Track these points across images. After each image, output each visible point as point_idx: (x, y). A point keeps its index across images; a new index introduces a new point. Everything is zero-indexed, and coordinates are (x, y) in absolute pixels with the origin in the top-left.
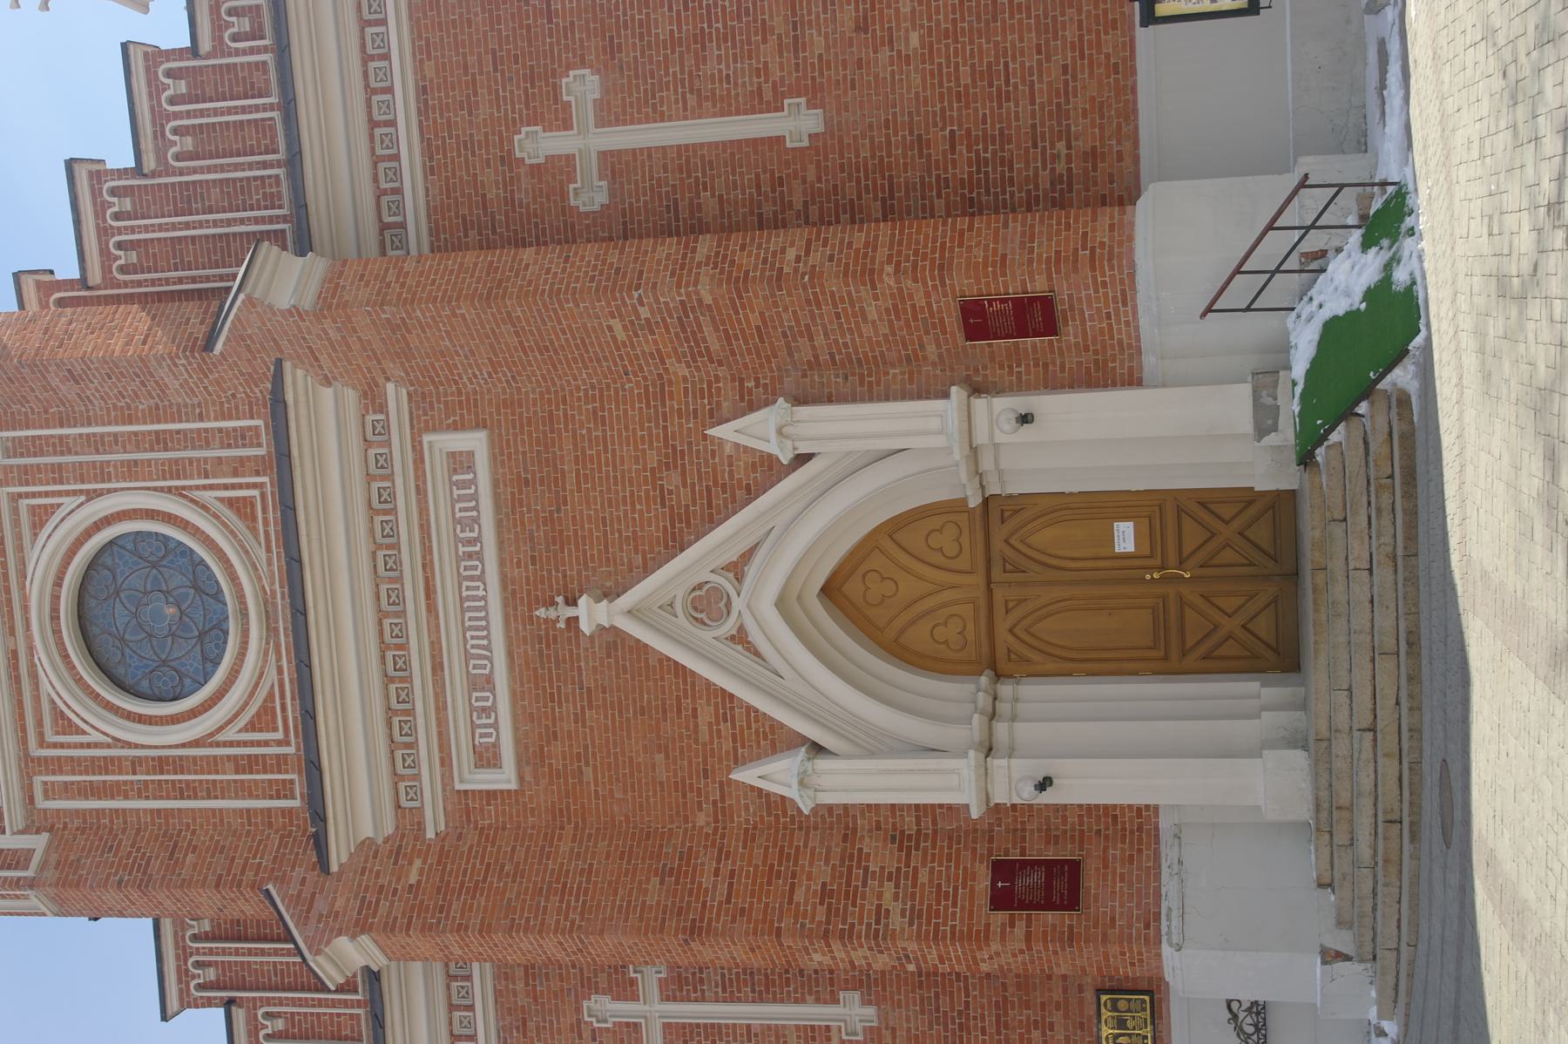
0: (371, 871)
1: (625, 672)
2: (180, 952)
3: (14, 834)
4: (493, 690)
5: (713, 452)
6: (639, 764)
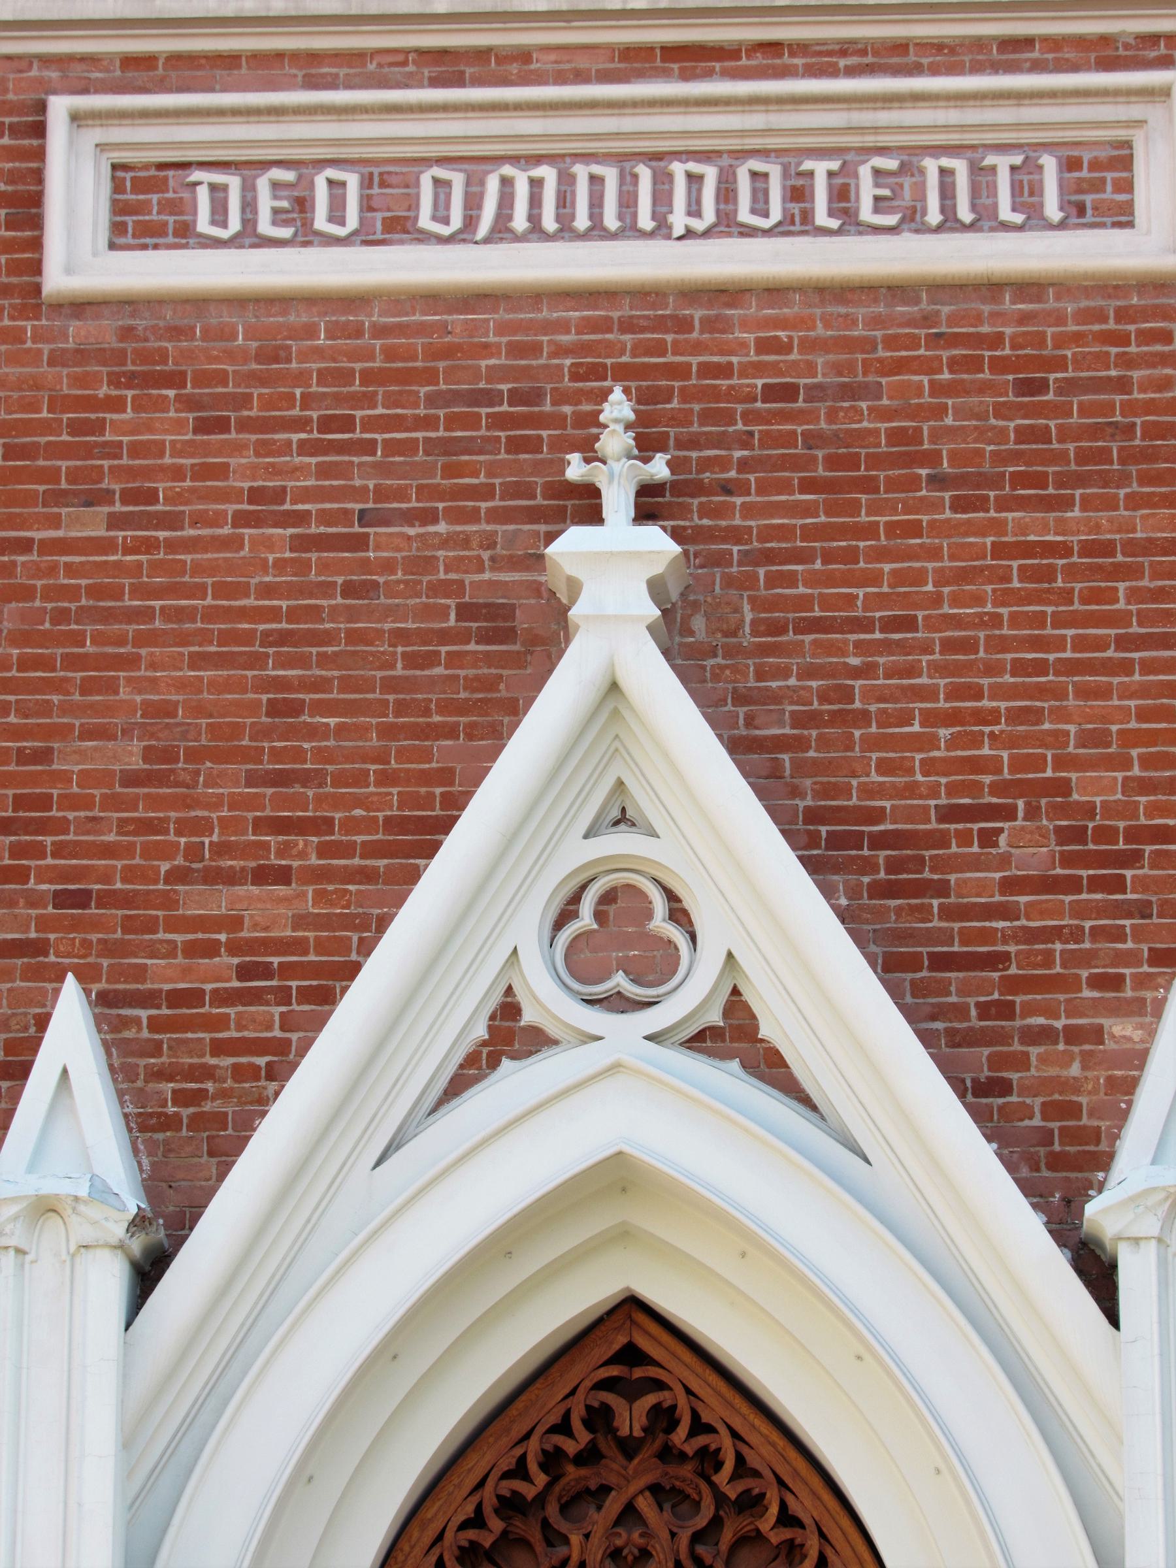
1: (411, 661)
4: (364, 237)
5: (1116, 982)
6: (111, 687)
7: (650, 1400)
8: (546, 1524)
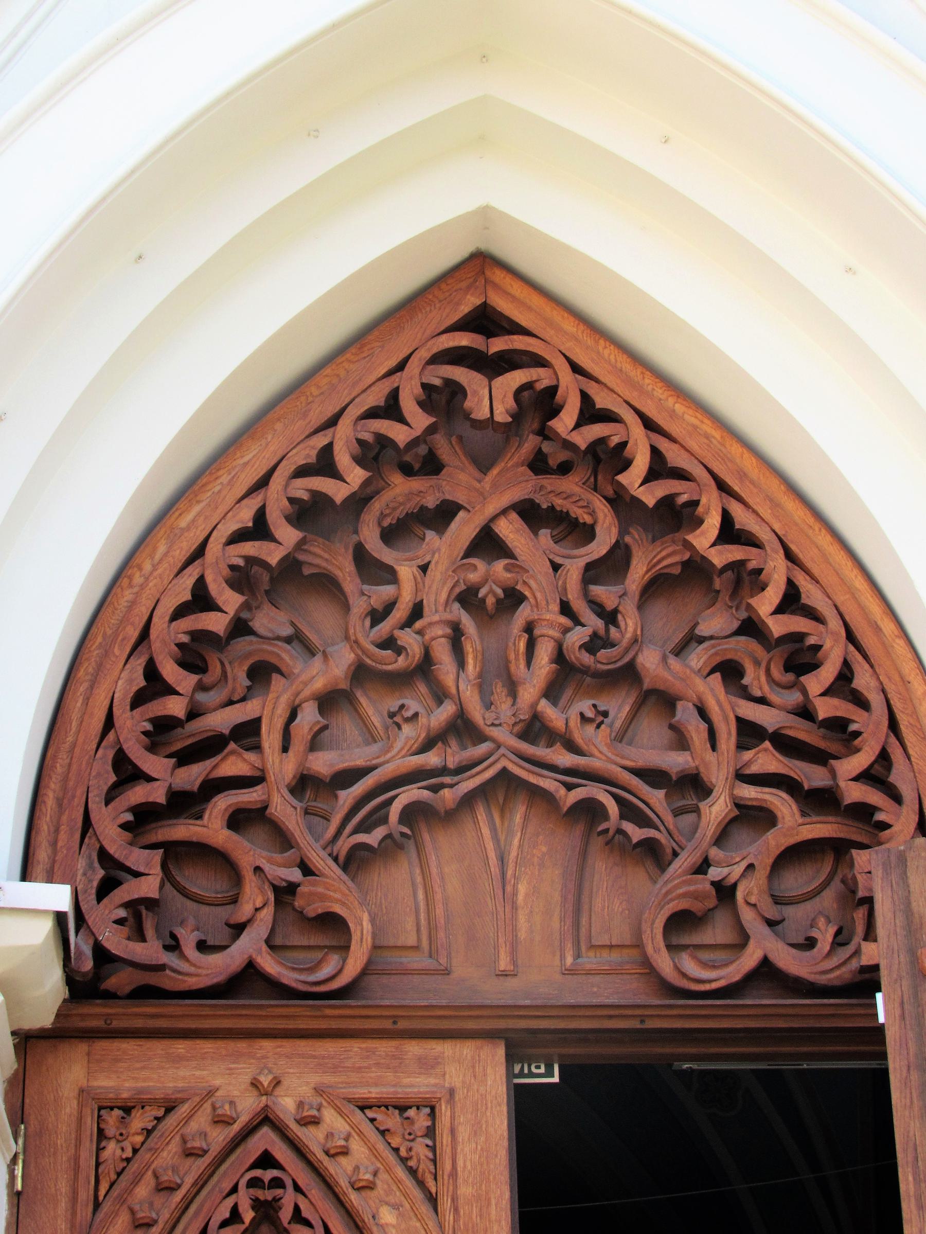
7: (517, 378)
8: (361, 556)
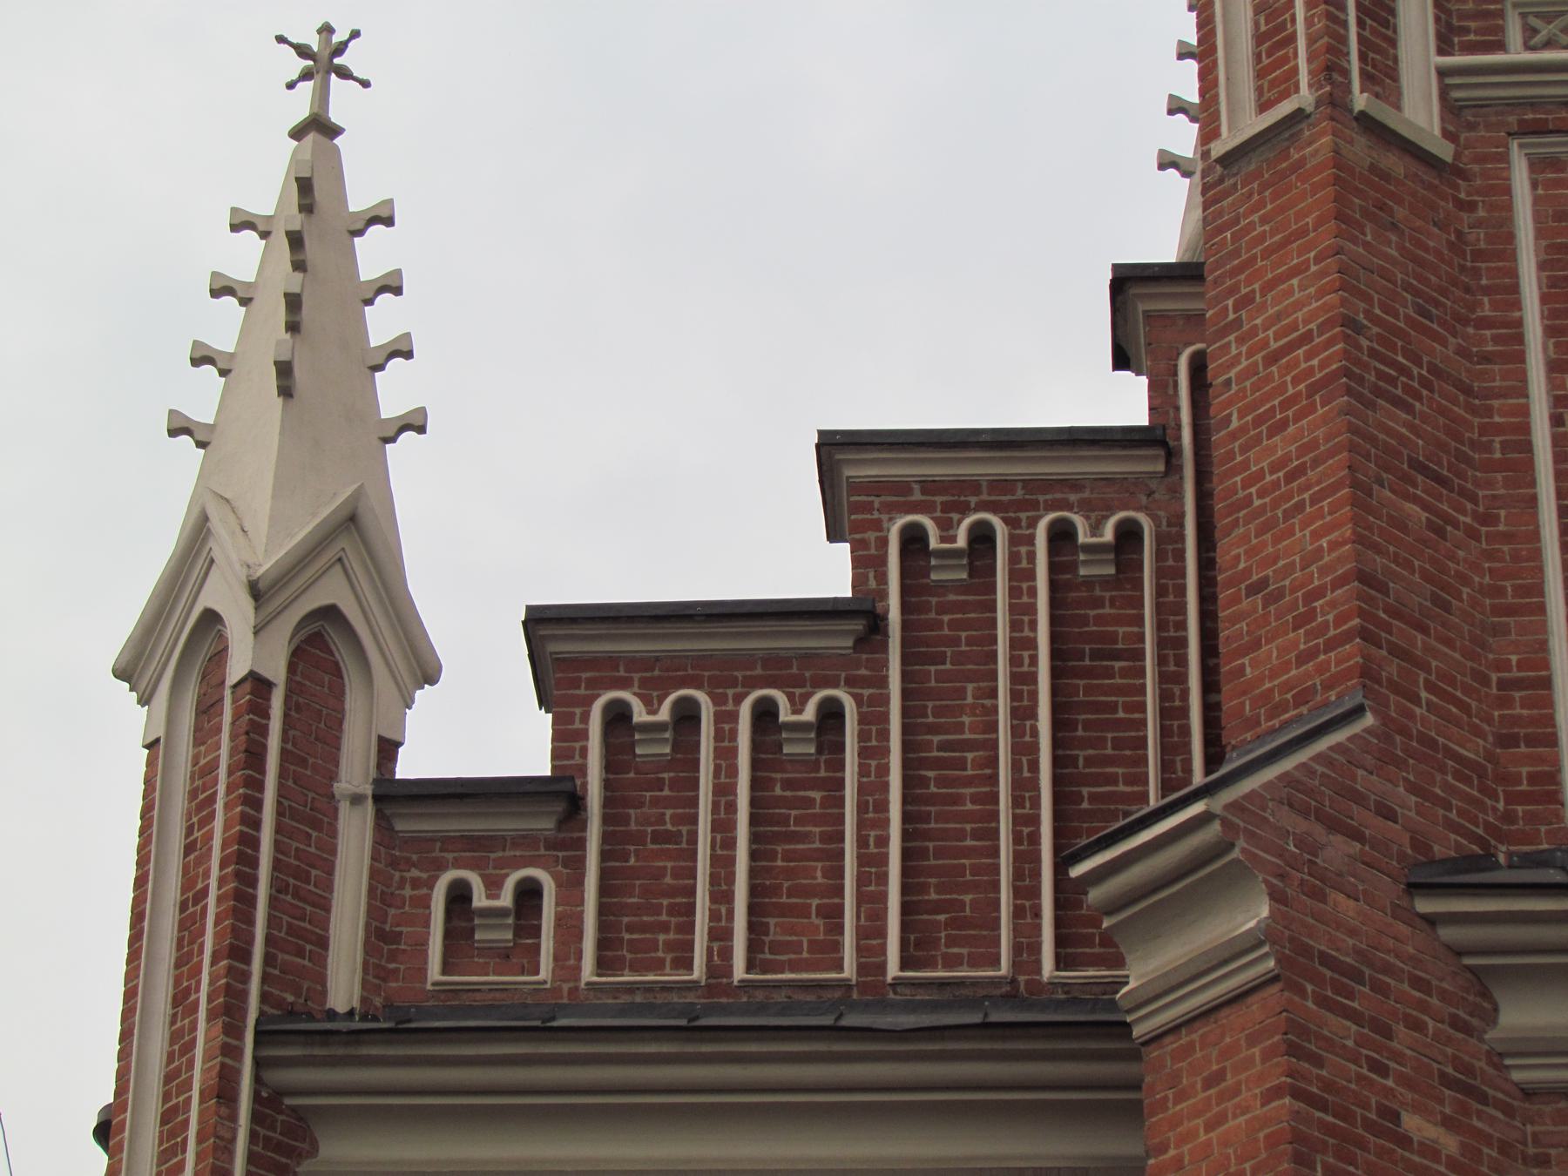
0: (1423, 1007)
2: (1020, 494)
3: (1442, 73)
